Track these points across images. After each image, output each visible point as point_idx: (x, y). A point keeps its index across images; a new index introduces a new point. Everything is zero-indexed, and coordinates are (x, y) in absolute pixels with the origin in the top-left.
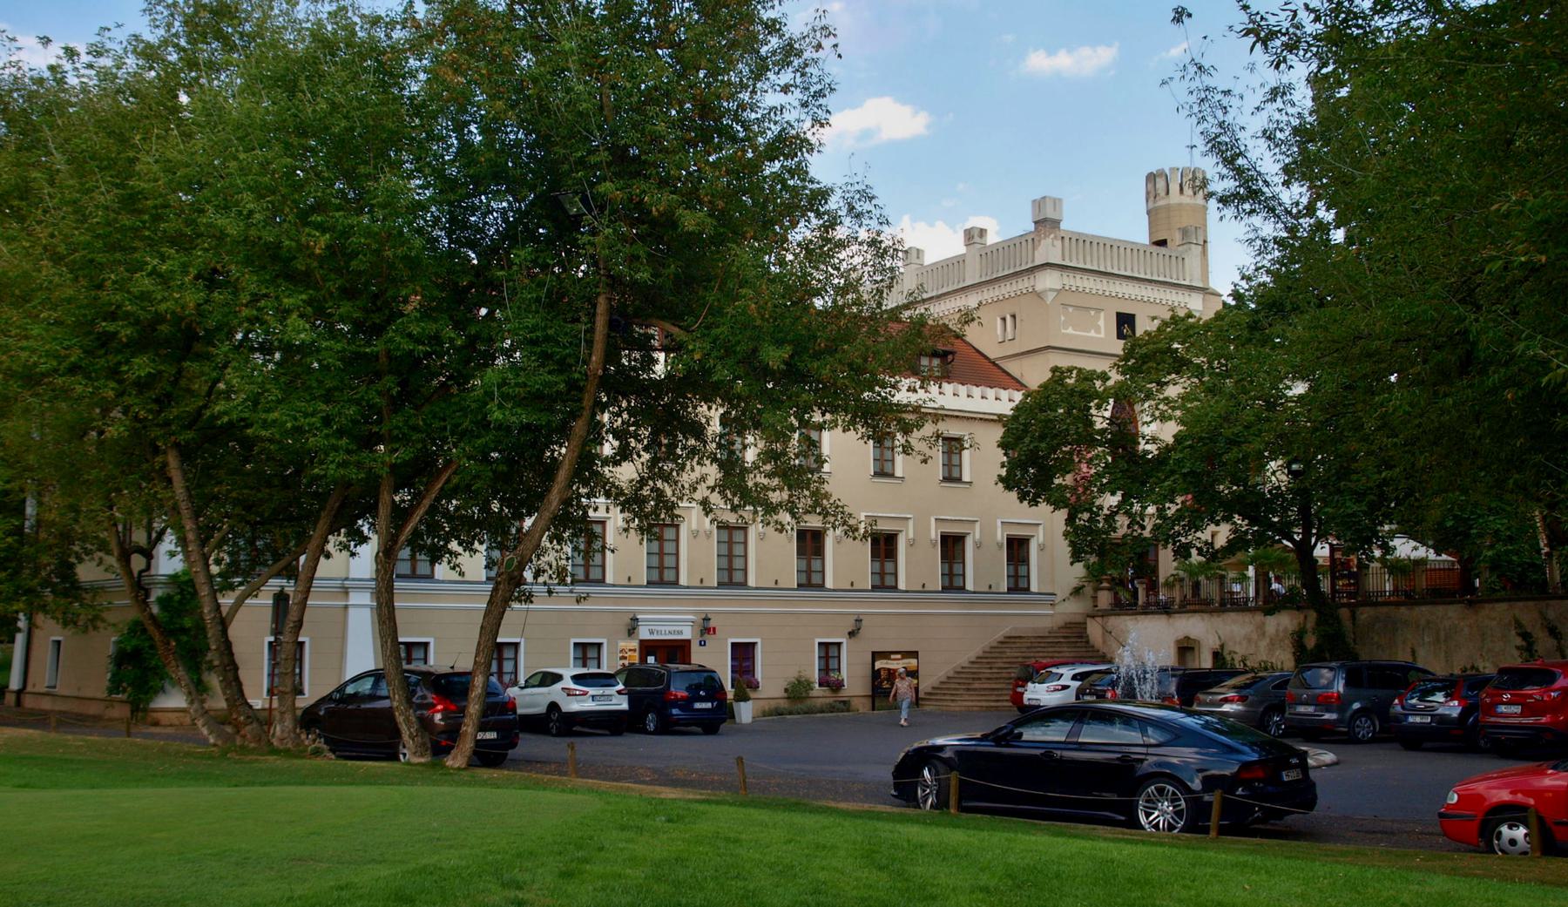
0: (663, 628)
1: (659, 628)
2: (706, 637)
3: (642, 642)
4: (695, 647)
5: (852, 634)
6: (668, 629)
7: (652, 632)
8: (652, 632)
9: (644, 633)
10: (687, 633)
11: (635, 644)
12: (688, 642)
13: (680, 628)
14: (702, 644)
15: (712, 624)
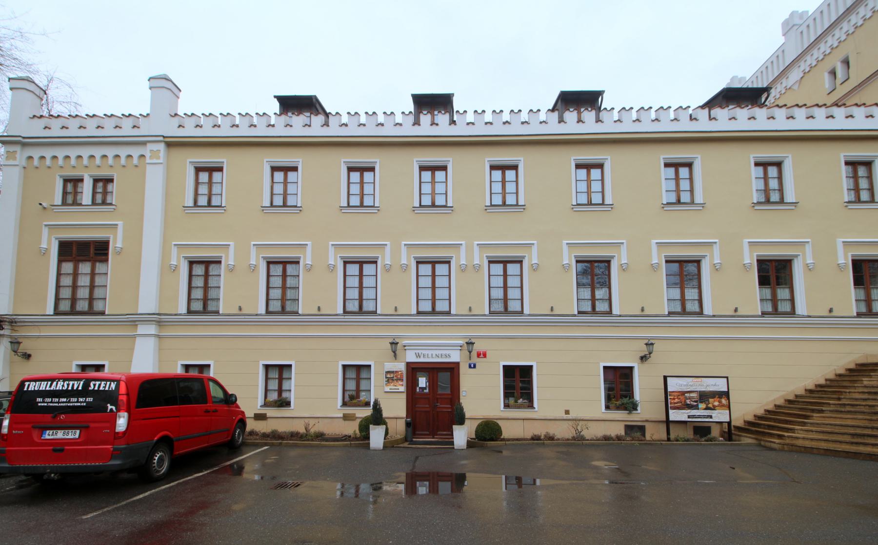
0: (430, 352)
1: (424, 352)
2: (475, 359)
3: (408, 364)
4: (464, 370)
5: (643, 358)
6: (434, 352)
7: (418, 356)
8: (418, 356)
9: (411, 357)
10: (455, 357)
11: (401, 367)
12: (458, 364)
13: (447, 352)
14: (473, 366)
15: (479, 346)
